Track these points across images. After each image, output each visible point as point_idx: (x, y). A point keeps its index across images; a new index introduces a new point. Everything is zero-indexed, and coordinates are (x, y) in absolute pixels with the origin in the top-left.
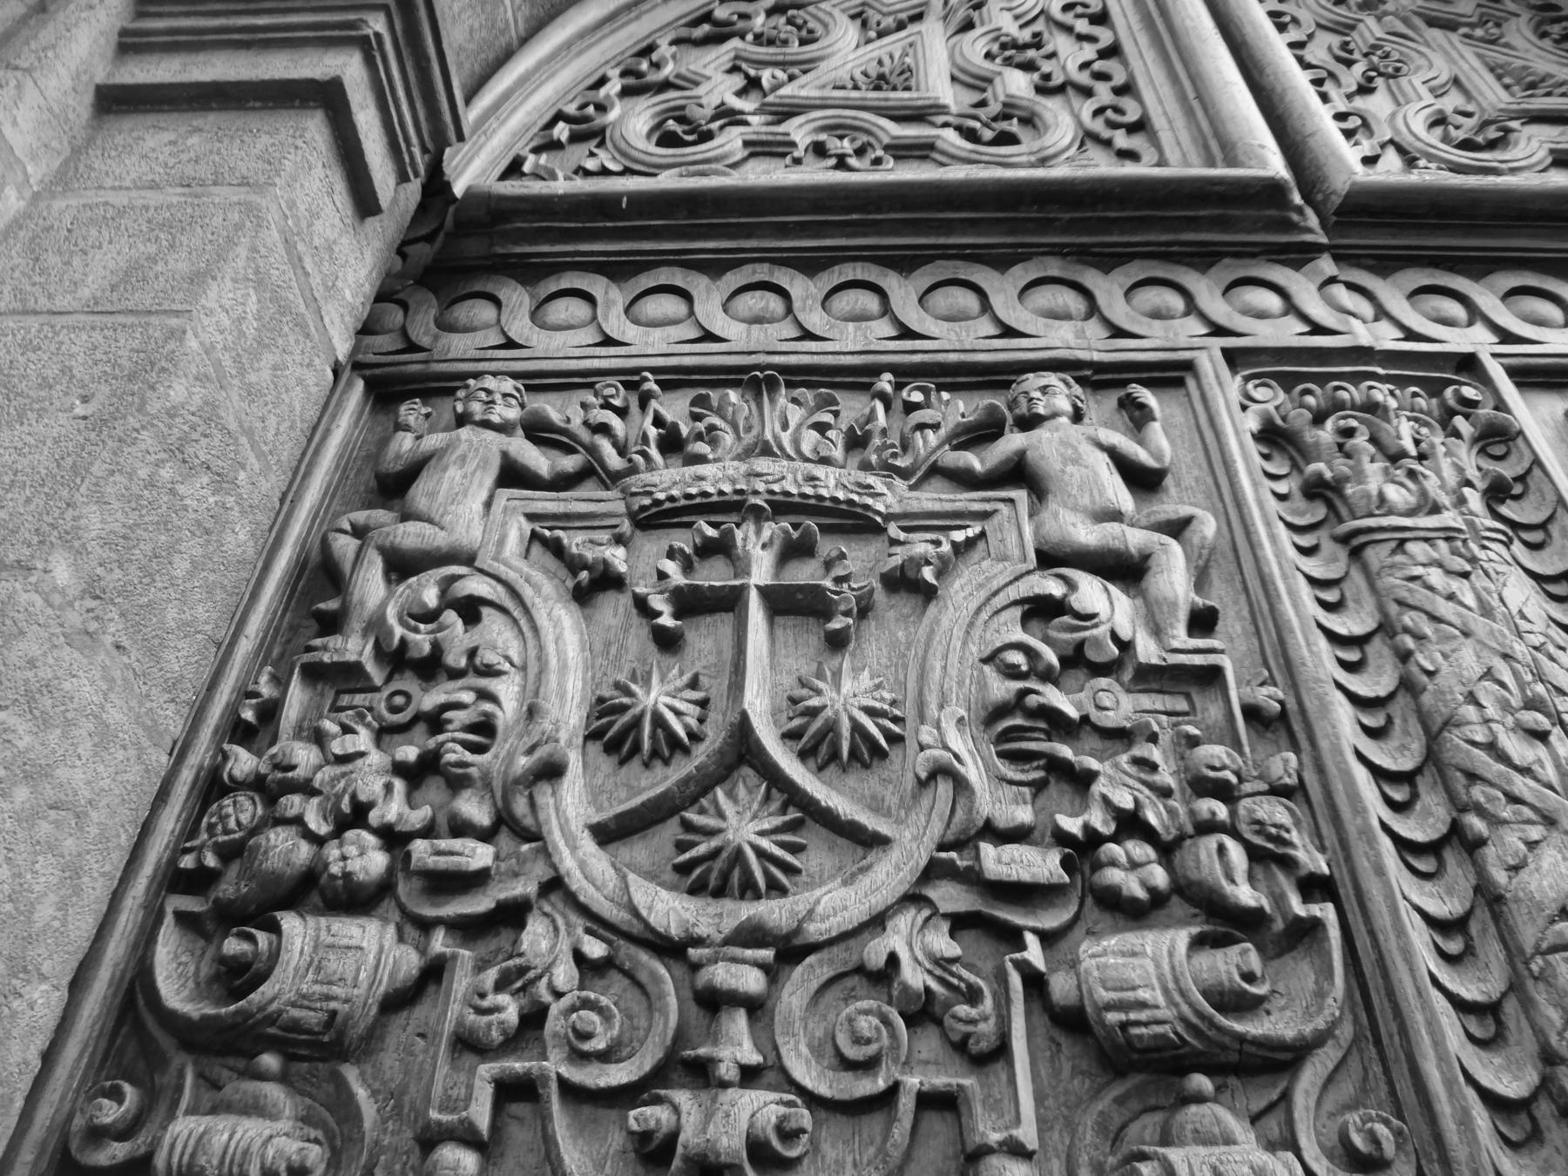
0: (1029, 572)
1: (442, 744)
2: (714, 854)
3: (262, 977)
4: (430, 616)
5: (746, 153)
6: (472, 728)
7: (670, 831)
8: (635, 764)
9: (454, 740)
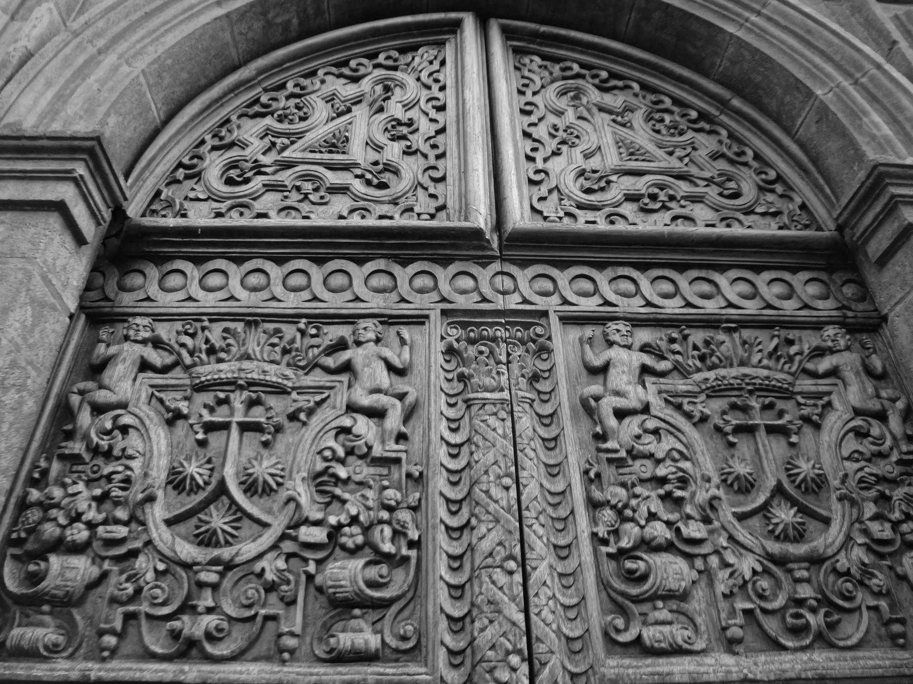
0: (342, 415)
2: (207, 531)
3: (43, 579)
4: (108, 433)
5: (264, 189)
6: (122, 481)
7: (194, 521)
8: (184, 494)
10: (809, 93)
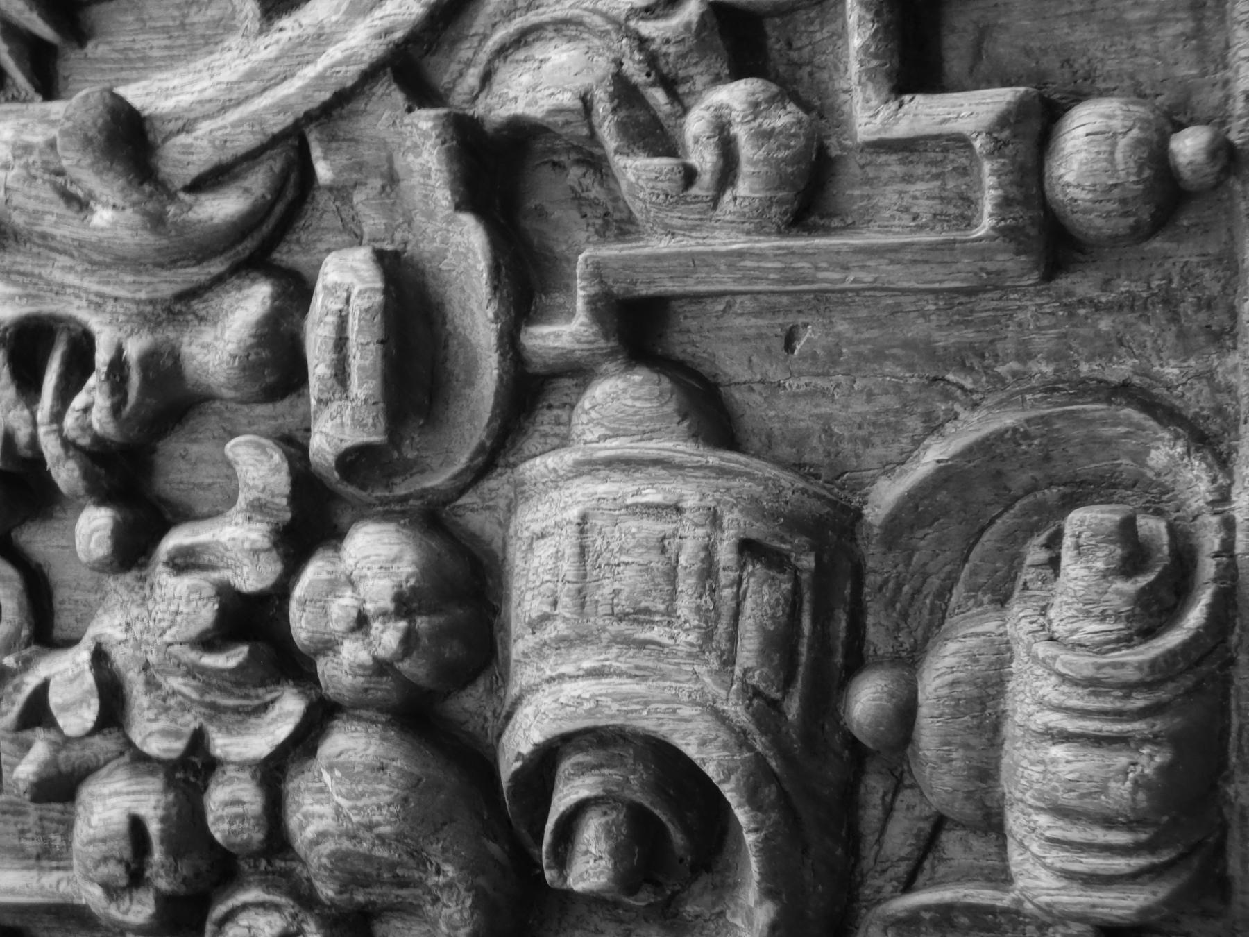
1: (68, 444)
9: (57, 417)
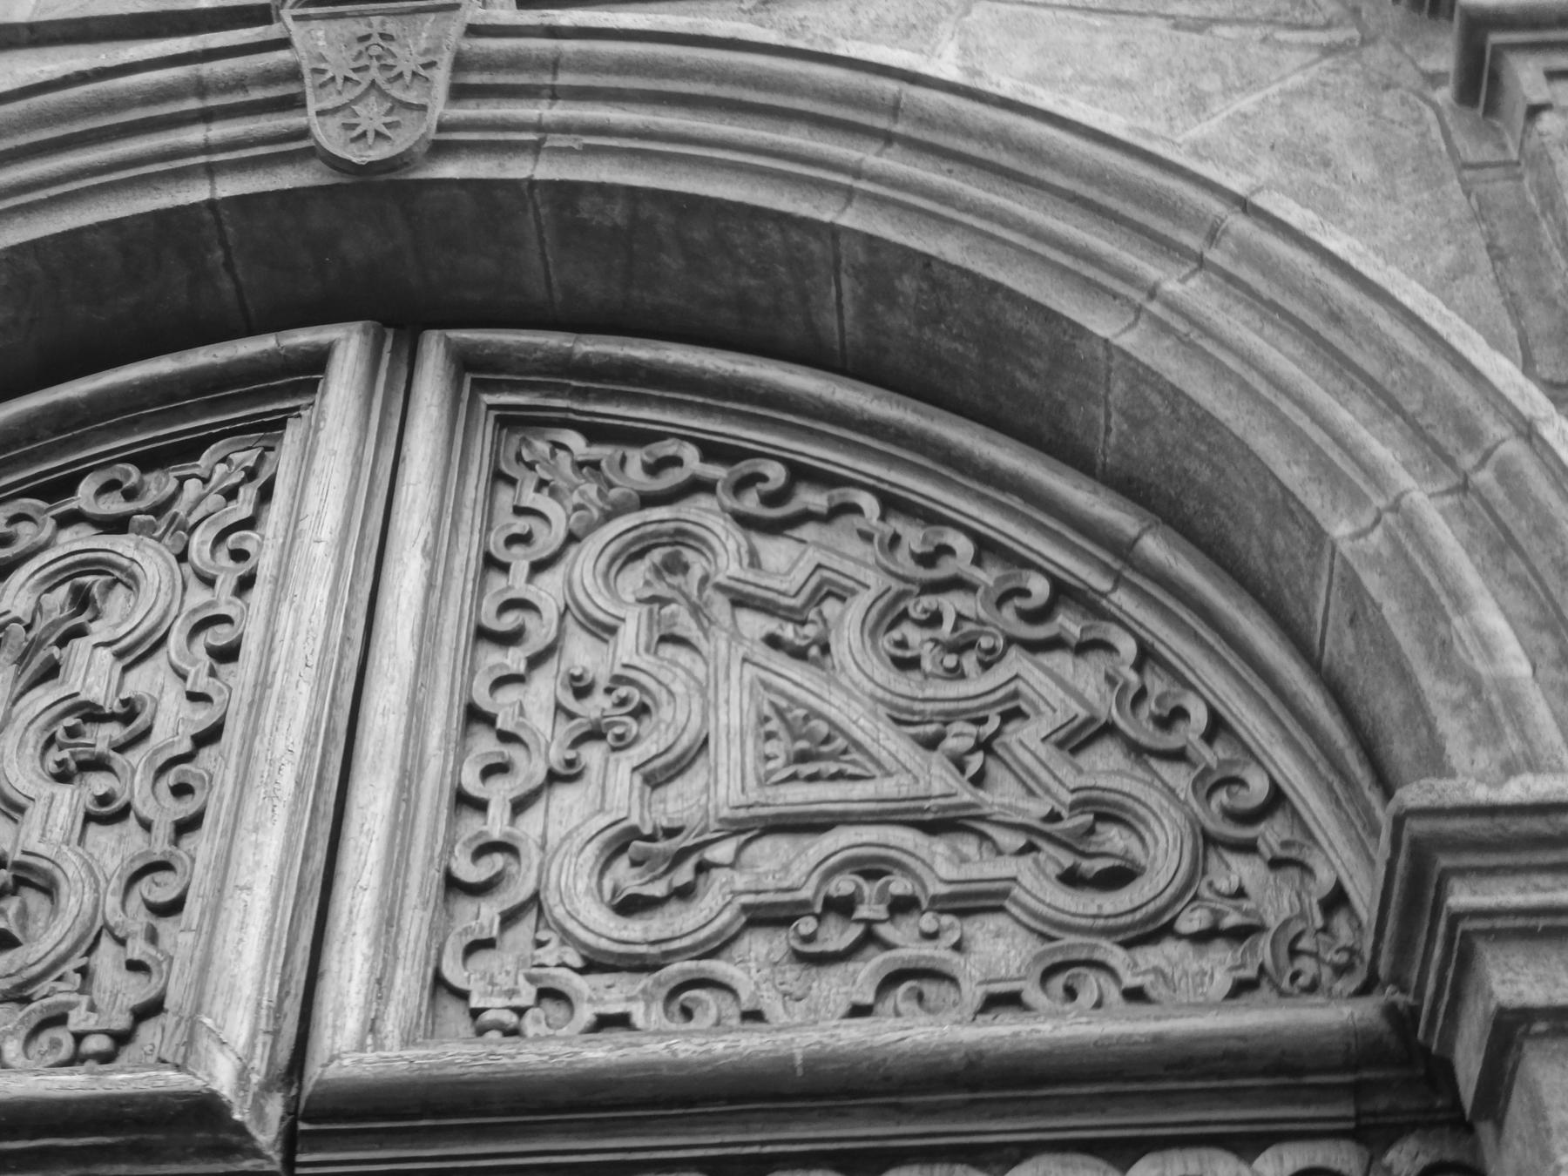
10: (1318, 535)
